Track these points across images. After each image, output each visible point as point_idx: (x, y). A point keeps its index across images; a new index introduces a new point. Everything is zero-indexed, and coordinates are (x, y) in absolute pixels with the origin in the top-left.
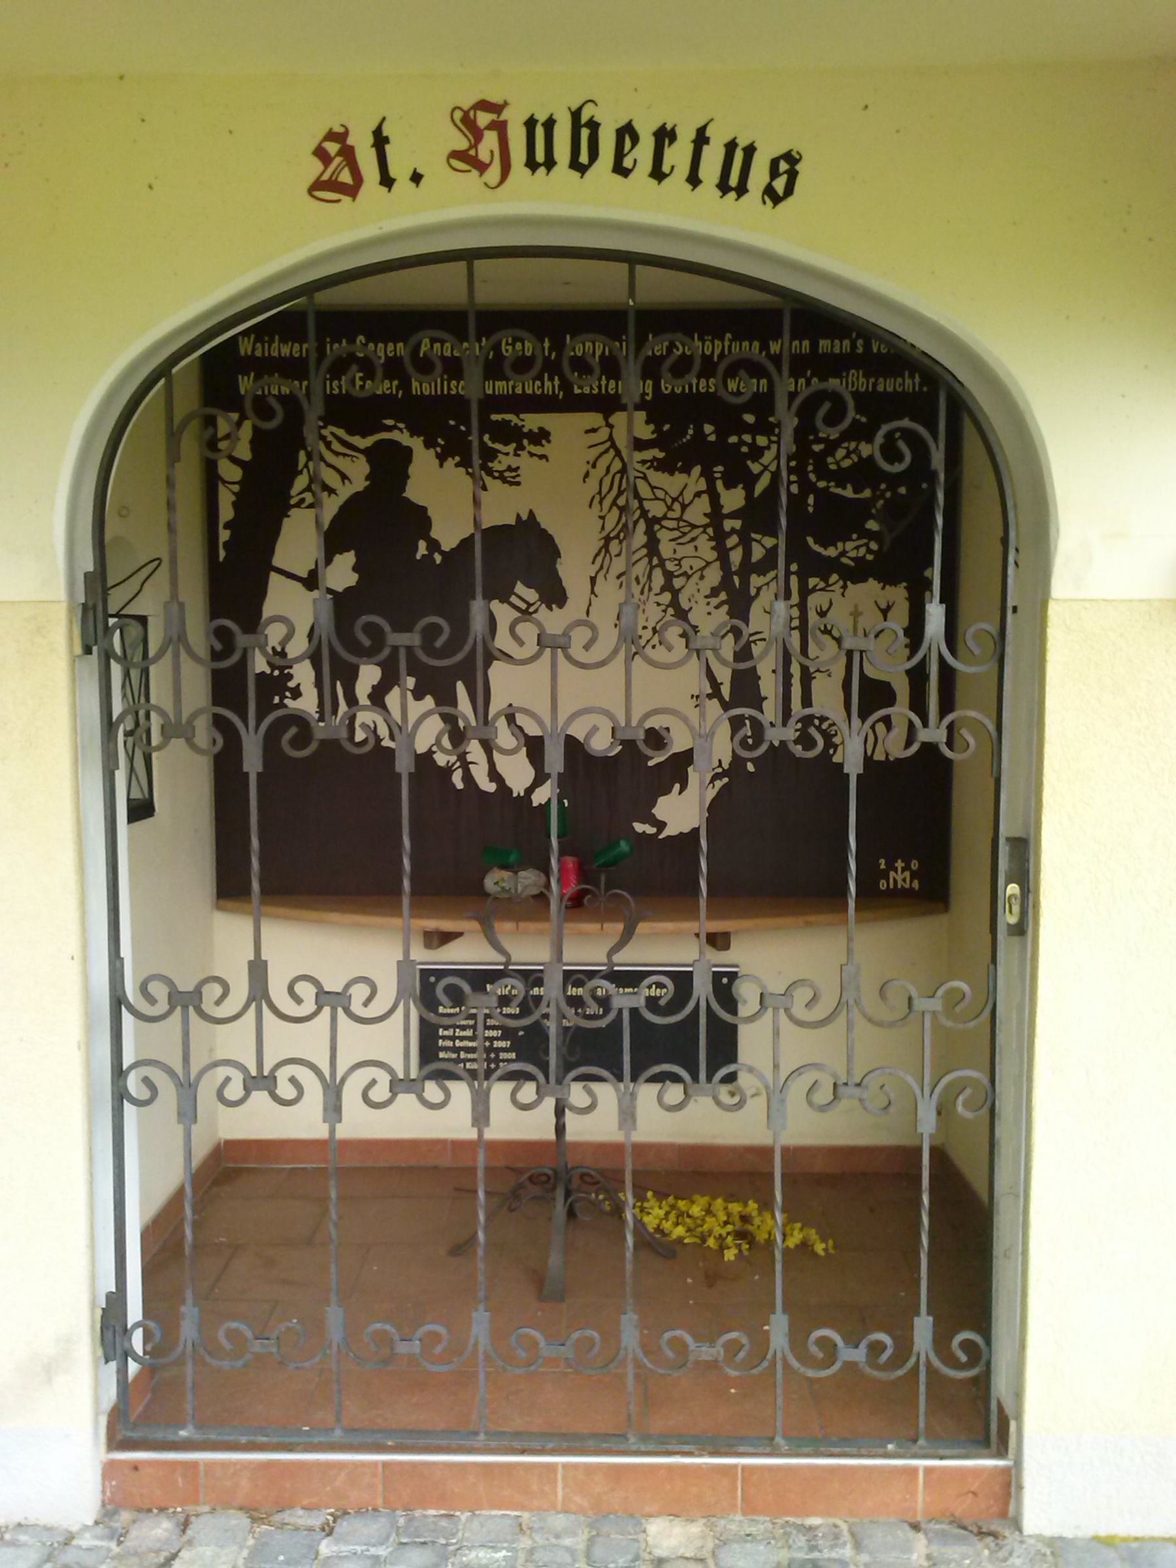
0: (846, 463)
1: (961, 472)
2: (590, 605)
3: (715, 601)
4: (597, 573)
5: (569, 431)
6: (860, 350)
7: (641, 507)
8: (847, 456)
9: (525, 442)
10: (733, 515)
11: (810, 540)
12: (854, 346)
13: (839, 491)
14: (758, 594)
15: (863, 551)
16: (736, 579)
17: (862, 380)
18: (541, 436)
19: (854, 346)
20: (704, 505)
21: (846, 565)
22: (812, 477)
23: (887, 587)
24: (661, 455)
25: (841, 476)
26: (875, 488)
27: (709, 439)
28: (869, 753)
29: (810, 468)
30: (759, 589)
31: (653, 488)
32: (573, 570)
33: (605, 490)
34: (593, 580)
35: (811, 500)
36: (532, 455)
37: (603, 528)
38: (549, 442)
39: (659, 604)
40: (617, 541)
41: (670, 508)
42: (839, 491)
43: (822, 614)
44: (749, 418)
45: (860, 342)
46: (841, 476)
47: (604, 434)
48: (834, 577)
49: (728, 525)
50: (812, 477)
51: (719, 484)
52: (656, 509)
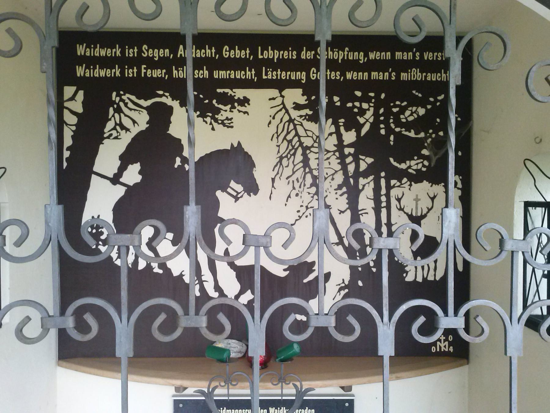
0: (411, 119)
1: (472, 125)
2: (271, 193)
3: (340, 192)
4: (275, 176)
5: (260, 99)
6: (418, 58)
7: (299, 140)
8: (411, 115)
9: (236, 104)
10: (349, 146)
11: (392, 160)
12: (390, 76)
13: (407, 133)
14: (363, 188)
15: (420, 166)
16: (352, 180)
17: (419, 74)
18: (245, 101)
19: (390, 76)
20: (334, 140)
21: (411, 173)
22: (393, 126)
23: (434, 185)
24: (310, 113)
25: (408, 126)
26: (426, 132)
27: (336, 104)
28: (425, 276)
29: (391, 121)
30: (364, 186)
31: (306, 130)
32: (262, 174)
33: (279, 132)
34: (273, 180)
35: (392, 138)
36: (240, 111)
37: (279, 152)
38: (249, 104)
39: (309, 193)
40: (286, 159)
41: (315, 142)
42: (407, 133)
43: (399, 200)
44: (358, 94)
45: (418, 54)
46: (408, 126)
47: (279, 101)
48: (405, 180)
49: (347, 151)
50: (393, 126)
51: (342, 129)
52: (308, 142)
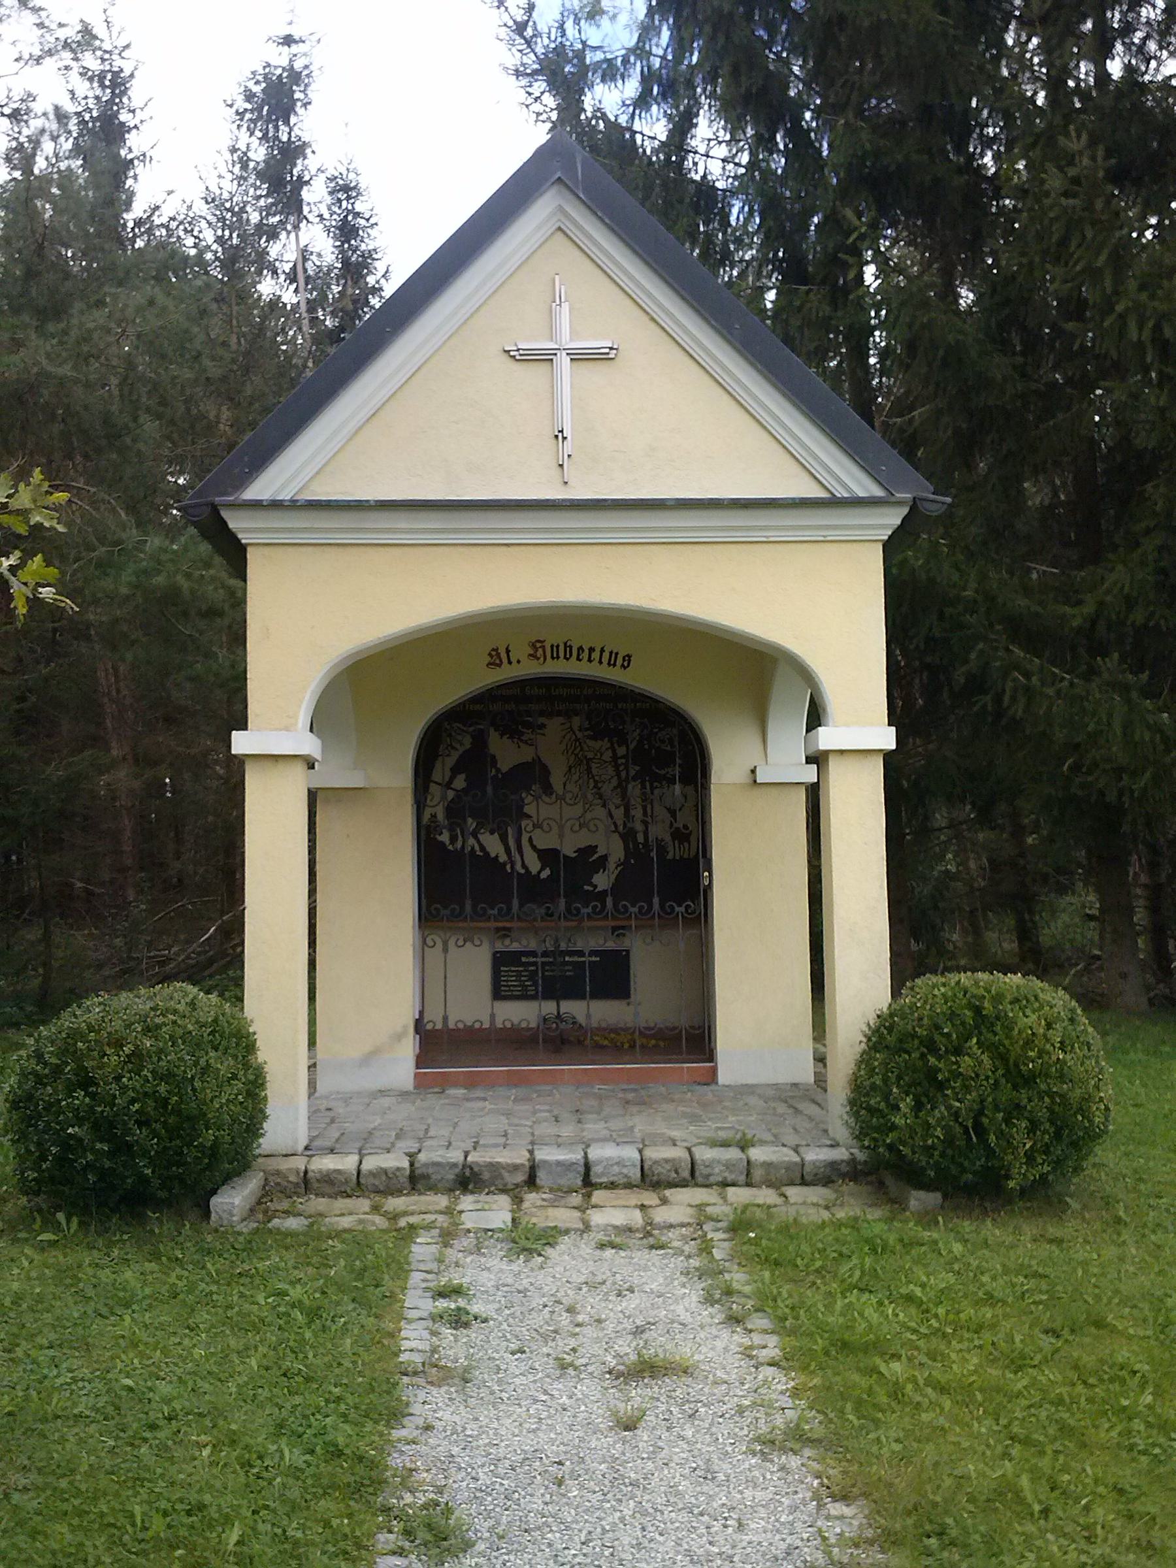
10: (622, 757)
18: (543, 726)
20: (610, 753)
32: (557, 780)
34: (565, 785)
47: (568, 725)
52: (590, 755)
